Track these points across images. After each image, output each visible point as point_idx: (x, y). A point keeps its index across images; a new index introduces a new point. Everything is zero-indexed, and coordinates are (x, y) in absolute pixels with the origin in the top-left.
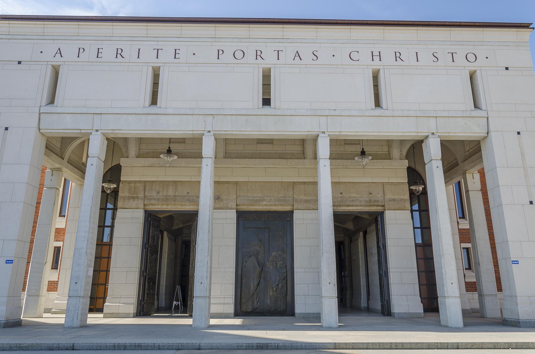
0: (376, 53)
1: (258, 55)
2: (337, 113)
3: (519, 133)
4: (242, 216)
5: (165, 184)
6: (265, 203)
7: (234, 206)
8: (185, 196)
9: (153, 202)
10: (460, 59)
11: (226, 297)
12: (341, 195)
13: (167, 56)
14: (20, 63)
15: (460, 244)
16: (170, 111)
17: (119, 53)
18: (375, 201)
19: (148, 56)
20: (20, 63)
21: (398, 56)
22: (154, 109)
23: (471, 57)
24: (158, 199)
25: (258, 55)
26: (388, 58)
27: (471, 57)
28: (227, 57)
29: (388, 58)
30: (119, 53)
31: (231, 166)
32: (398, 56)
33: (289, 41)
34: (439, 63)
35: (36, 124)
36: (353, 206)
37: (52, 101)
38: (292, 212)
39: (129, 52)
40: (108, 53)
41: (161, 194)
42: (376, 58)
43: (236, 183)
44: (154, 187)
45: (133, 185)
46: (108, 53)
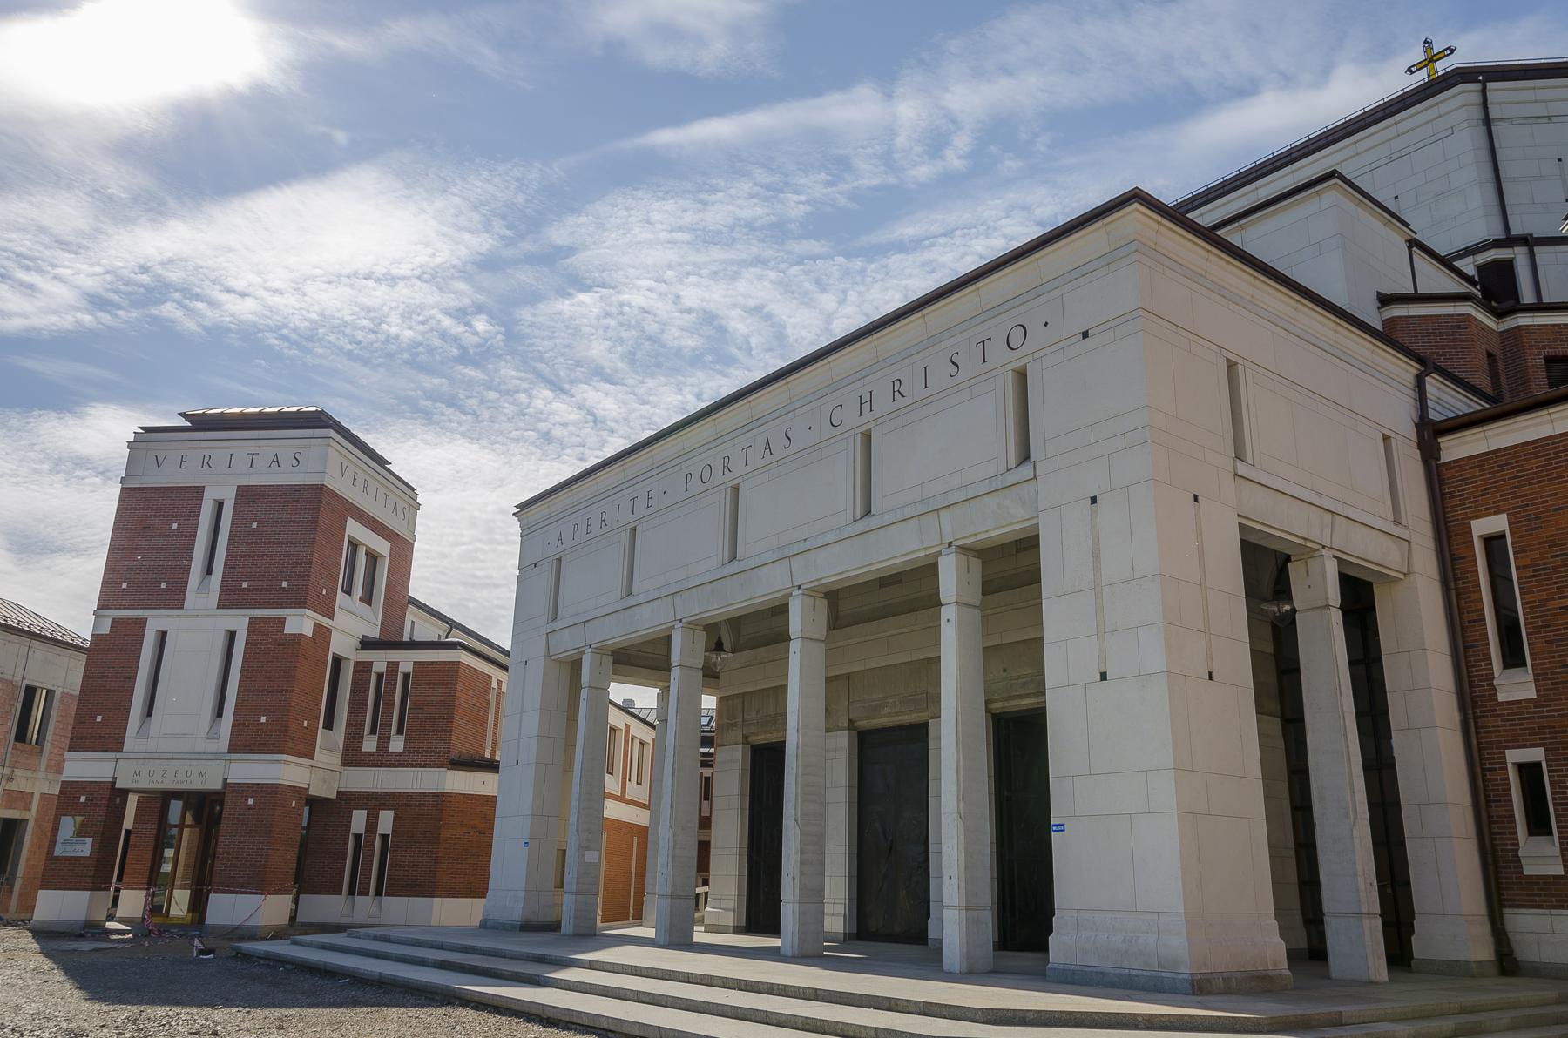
7: (846, 725)
10: (997, 351)
11: (837, 901)
12: (1004, 675)
15: (711, 814)
26: (883, 403)
28: (695, 485)
31: (839, 644)
34: (962, 375)
35: (542, 651)
42: (866, 407)
43: (849, 676)
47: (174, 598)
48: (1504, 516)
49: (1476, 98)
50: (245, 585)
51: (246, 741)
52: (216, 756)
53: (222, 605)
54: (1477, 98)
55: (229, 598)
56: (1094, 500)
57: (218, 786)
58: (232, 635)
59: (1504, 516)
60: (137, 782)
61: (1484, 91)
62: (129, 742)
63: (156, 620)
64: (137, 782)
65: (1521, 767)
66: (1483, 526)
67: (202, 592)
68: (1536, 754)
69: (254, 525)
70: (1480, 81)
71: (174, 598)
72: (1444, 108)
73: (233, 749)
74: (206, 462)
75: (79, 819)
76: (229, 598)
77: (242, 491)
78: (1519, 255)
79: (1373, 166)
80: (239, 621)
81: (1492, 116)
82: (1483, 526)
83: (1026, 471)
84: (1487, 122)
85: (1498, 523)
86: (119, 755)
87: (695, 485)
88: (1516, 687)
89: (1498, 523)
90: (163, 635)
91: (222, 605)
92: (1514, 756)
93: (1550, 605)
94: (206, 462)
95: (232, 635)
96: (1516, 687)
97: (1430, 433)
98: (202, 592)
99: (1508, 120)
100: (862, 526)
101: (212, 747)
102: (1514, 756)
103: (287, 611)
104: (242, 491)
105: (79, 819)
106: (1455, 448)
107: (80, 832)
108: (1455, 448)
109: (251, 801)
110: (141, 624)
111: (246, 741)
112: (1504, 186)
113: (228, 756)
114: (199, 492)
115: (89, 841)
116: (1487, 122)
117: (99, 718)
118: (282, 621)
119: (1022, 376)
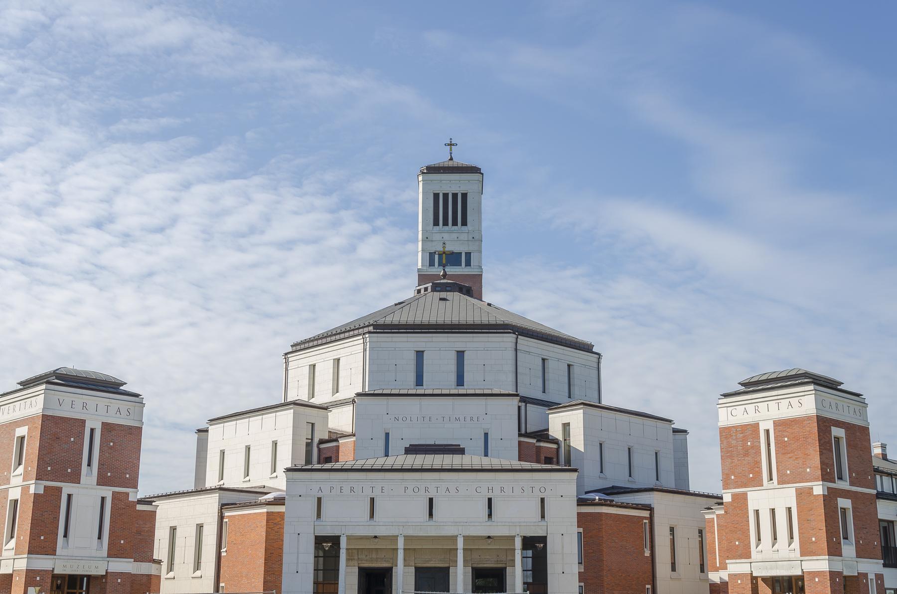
1: (426, 490)
2: (467, 524)
3: (562, 535)
4: (417, 569)
5: (370, 550)
6: (432, 562)
7: (413, 565)
8: (383, 558)
9: (363, 562)
10: (536, 490)
12: (479, 557)
14: (300, 496)
16: (381, 524)
17: (352, 489)
18: (501, 561)
20: (300, 496)
21: (502, 490)
22: (372, 523)
24: (367, 560)
25: (426, 490)
26: (497, 491)
28: (410, 491)
29: (497, 491)
30: (352, 489)
32: (502, 490)
33: (443, 481)
36: (487, 564)
38: (449, 568)
40: (346, 490)
41: (368, 557)
42: (491, 491)
43: (414, 549)
44: (363, 552)
45: (350, 551)
46: (346, 490)
47: (75, 478)
48: (582, 529)
50: (109, 474)
51: (115, 552)
53: (99, 483)
54: (514, 340)
55: (102, 481)
56: (562, 535)
58: (103, 499)
59: (582, 529)
60: (65, 570)
61: (517, 338)
63: (67, 488)
64: (65, 570)
67: (89, 476)
69: (112, 444)
70: (516, 334)
71: (75, 478)
72: (505, 339)
73: (109, 556)
74: (84, 406)
75: (38, 588)
76: (102, 481)
77: (105, 425)
79: (478, 349)
80: (107, 492)
81: (518, 348)
84: (516, 350)
86: (55, 557)
87: (410, 491)
90: (69, 496)
91: (99, 483)
93: (590, 551)
94: (84, 406)
95: (103, 499)
98: (89, 476)
99: (519, 350)
100: (489, 523)
104: (105, 425)
105: (38, 588)
109: (119, 580)
110: (60, 490)
111: (115, 552)
112: (518, 375)
113: (108, 559)
114: (83, 422)
116: (516, 350)
117: (42, 538)
118: (127, 494)
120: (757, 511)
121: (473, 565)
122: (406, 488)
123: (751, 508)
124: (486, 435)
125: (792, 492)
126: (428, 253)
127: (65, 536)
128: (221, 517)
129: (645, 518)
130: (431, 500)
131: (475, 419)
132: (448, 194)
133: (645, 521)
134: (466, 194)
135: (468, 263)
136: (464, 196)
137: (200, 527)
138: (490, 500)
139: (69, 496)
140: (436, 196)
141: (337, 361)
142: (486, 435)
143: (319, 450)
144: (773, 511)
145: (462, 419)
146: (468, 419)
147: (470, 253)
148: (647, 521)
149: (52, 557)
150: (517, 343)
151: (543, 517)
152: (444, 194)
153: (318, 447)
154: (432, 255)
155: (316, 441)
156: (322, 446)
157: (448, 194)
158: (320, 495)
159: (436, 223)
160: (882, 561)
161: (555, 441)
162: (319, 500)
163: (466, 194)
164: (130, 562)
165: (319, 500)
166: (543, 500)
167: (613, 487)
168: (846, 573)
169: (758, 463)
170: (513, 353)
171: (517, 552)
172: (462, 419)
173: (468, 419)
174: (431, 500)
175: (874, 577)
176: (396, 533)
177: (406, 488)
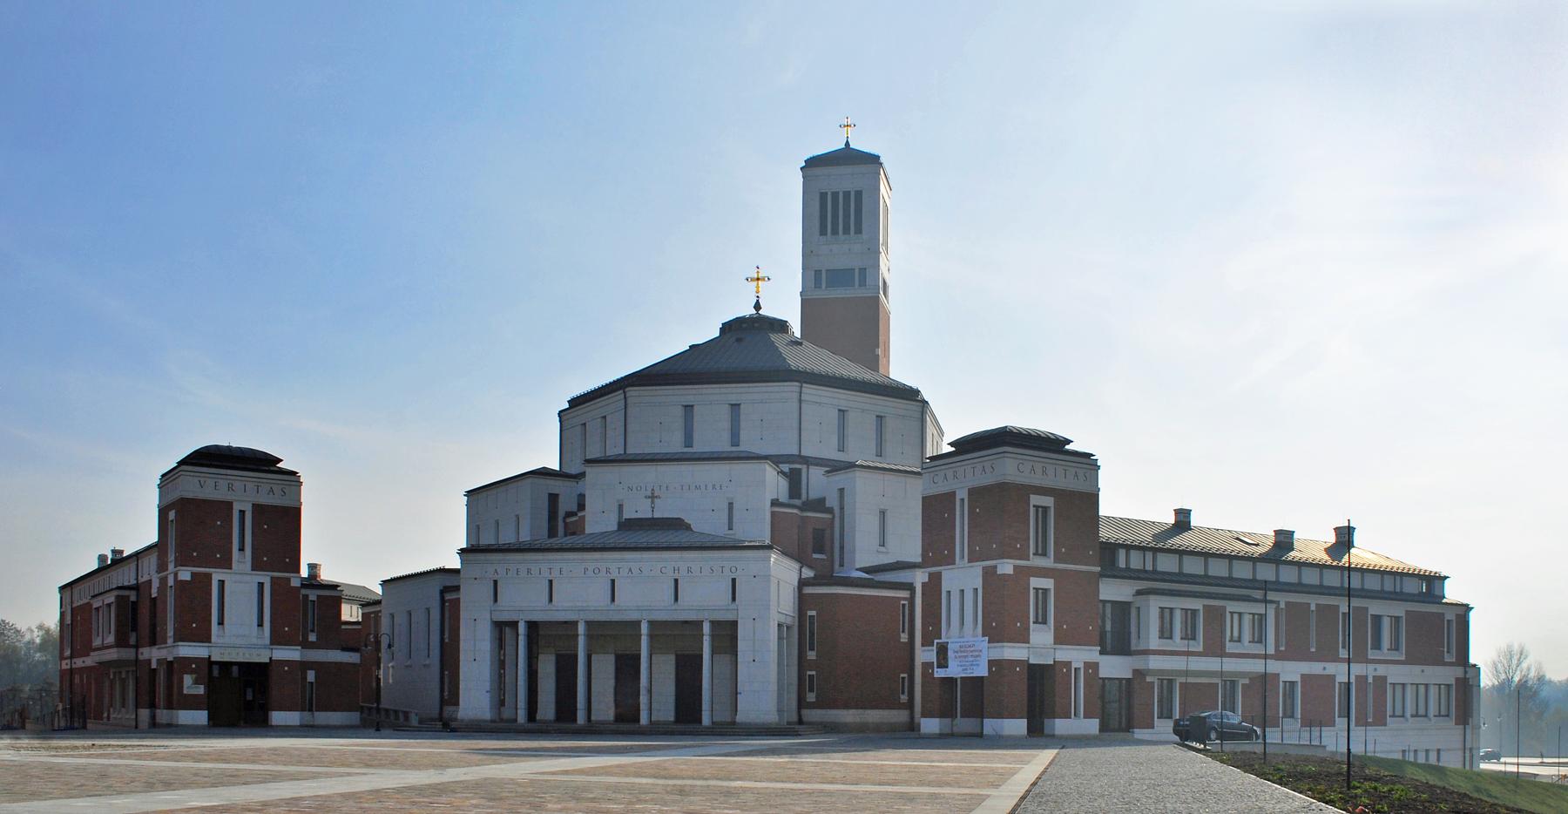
0: (676, 568)
1: (608, 571)
13: (555, 573)
17: (529, 571)
19: (546, 574)
23: (733, 569)
25: (608, 571)
26: (683, 571)
27: (733, 569)
28: (590, 573)
29: (683, 571)
30: (529, 571)
35: (489, 618)
37: (496, 600)
39: (535, 570)
40: (523, 573)
49: (798, 389)
51: (278, 639)
52: (265, 647)
57: (268, 661)
58: (261, 585)
61: (801, 387)
62: (214, 638)
65: (809, 675)
66: (810, 613)
68: (814, 673)
73: (272, 644)
75: (194, 676)
78: (804, 468)
80: (265, 578)
82: (810, 613)
83: (733, 606)
85: (813, 613)
86: (210, 645)
88: (812, 655)
89: (813, 613)
90: (222, 583)
92: (809, 673)
95: (261, 585)
96: (812, 655)
97: (802, 583)
99: (805, 401)
101: (260, 642)
102: (809, 673)
103: (292, 575)
106: (808, 590)
107: (196, 682)
108: (808, 590)
111: (278, 639)
113: (271, 647)
115: (202, 686)
116: (800, 401)
118: (289, 580)
119: (734, 580)
120: (949, 592)
121: (679, 652)
122: (586, 570)
123: (945, 587)
124: (731, 504)
125: (979, 571)
126: (813, 273)
127: (221, 623)
128: (443, 601)
129: (904, 599)
130: (613, 581)
131: (718, 487)
132: (838, 193)
133: (902, 602)
134: (861, 191)
135: (863, 283)
136: (859, 194)
137: (428, 610)
138: (676, 581)
139: (222, 583)
140: (823, 196)
141: (735, 407)
142: (731, 504)
143: (566, 524)
144: (962, 591)
145: (703, 488)
146: (710, 488)
147: (865, 269)
148: (906, 602)
149: (207, 644)
150: (801, 393)
151: (734, 599)
152: (833, 193)
153: (564, 521)
154: (818, 273)
155: (561, 514)
156: (569, 520)
157: (838, 193)
158: (496, 577)
159: (823, 232)
160: (1099, 648)
161: (830, 511)
162: (495, 582)
163: (861, 191)
164: (297, 649)
165: (495, 582)
166: (734, 580)
167: (897, 562)
168: (1032, 661)
169: (953, 538)
170: (796, 405)
171: (705, 638)
172: (703, 488)
173: (710, 488)
174: (613, 581)
175: (1082, 666)
176: (639, 618)
177: (586, 570)
